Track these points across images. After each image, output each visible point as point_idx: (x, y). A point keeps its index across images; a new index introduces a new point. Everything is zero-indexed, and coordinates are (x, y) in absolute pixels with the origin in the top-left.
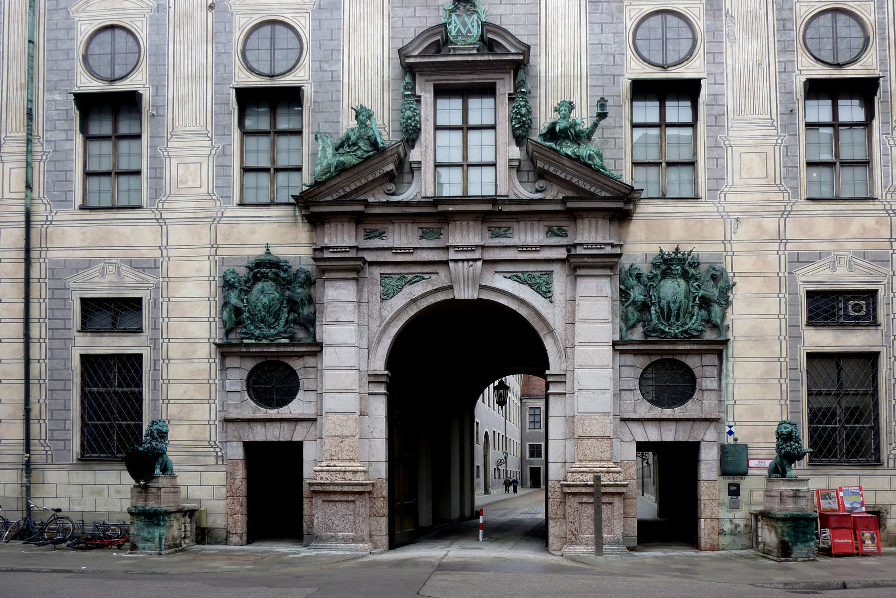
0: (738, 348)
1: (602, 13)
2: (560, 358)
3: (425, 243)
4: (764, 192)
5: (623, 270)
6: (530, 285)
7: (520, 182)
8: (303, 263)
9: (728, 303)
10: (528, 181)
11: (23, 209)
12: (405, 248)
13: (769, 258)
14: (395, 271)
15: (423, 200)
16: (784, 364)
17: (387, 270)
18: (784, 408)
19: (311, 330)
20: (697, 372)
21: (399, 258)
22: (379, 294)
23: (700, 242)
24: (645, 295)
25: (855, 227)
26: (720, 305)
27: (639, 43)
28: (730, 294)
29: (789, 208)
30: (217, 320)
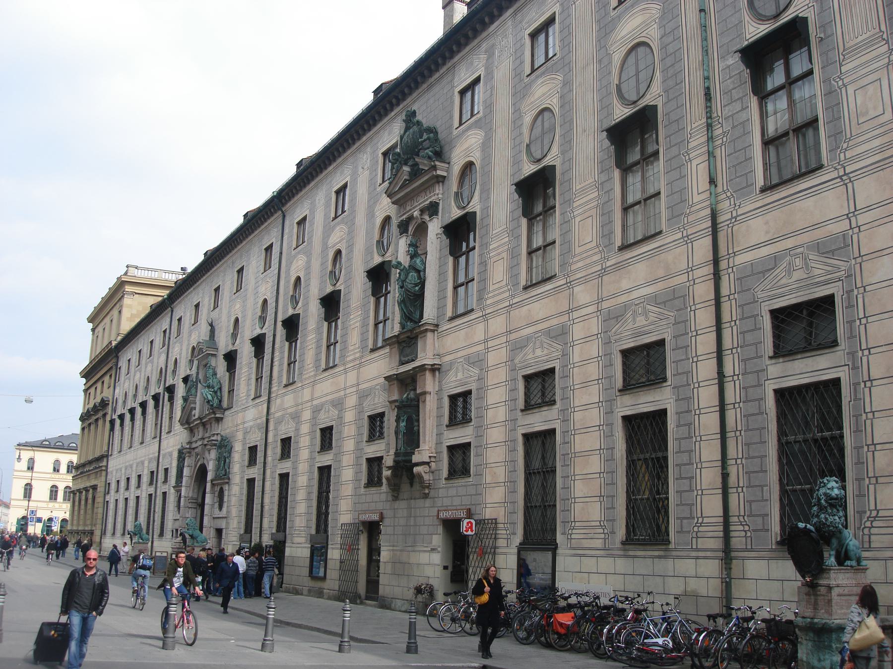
11: (708, 211)
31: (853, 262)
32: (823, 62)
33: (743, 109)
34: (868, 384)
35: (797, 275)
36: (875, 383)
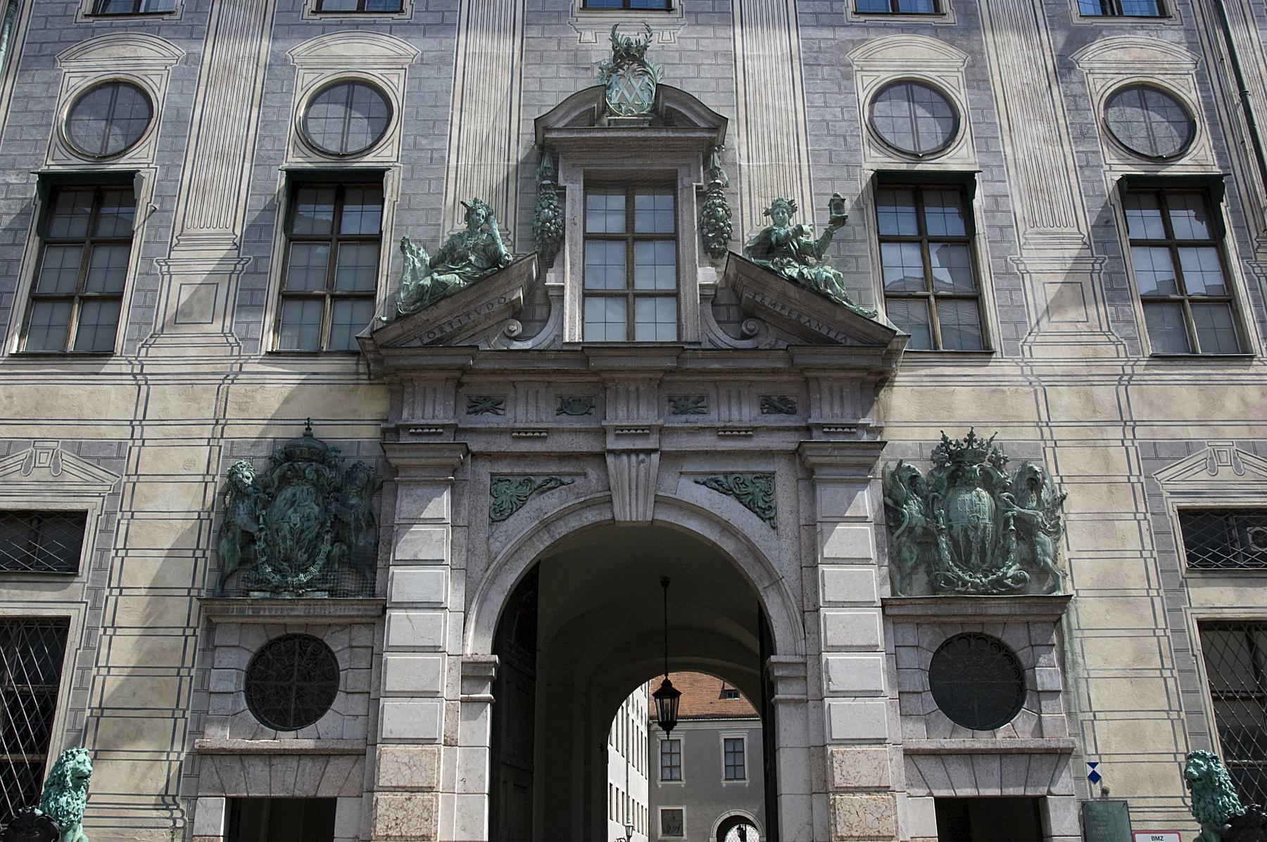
0: (1087, 612)
1: (823, 79)
2: (794, 632)
3: (567, 422)
4: (1086, 344)
5: (887, 471)
6: (738, 497)
7: (718, 322)
8: (364, 453)
9: (1057, 531)
10: (728, 322)
12: (534, 430)
13: (1111, 450)
14: (516, 470)
15: (566, 348)
16: (1164, 640)
17: (503, 468)
18: (1177, 724)
19: (368, 575)
20: (1023, 656)
21: (524, 447)
22: (486, 511)
23: (1004, 425)
24: (926, 516)
25: (1232, 402)
26: (1048, 533)
27: (878, 122)
28: (1059, 513)
29: (1128, 370)
30: (208, 553)
31: (125, 479)
32: (148, 235)
33: (13, 244)
34: (110, 631)
35: (36, 474)
36: (119, 631)
